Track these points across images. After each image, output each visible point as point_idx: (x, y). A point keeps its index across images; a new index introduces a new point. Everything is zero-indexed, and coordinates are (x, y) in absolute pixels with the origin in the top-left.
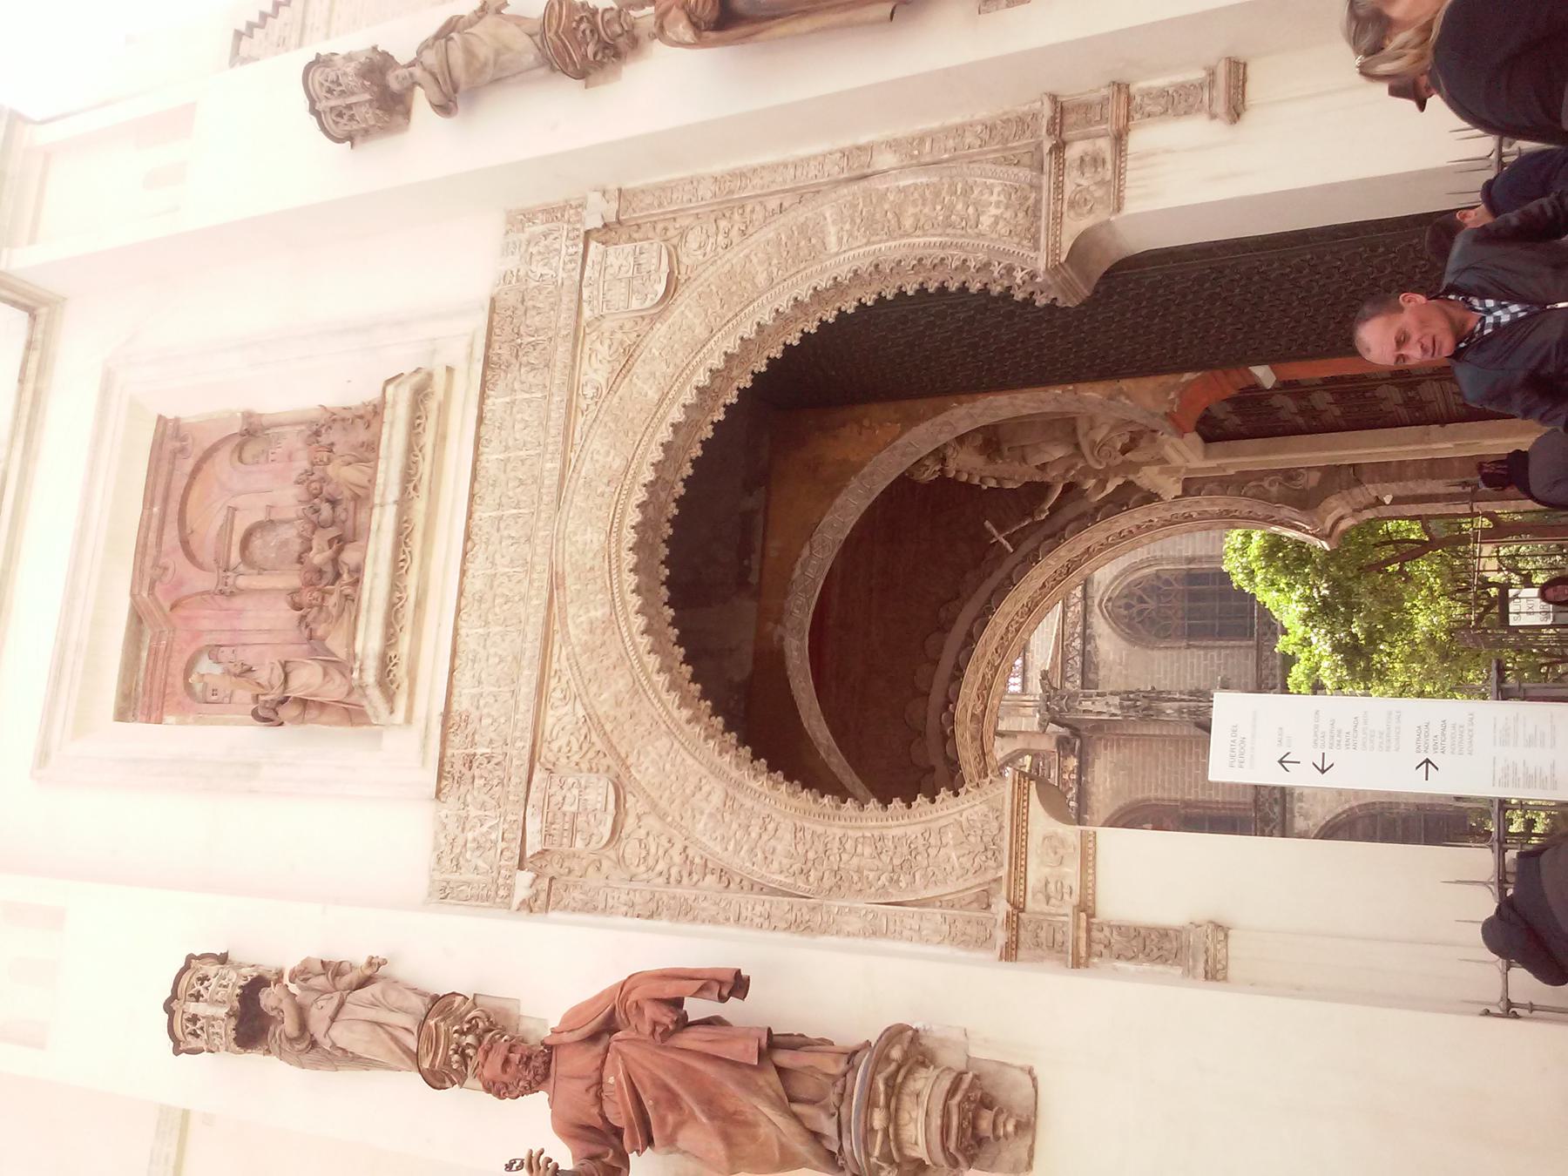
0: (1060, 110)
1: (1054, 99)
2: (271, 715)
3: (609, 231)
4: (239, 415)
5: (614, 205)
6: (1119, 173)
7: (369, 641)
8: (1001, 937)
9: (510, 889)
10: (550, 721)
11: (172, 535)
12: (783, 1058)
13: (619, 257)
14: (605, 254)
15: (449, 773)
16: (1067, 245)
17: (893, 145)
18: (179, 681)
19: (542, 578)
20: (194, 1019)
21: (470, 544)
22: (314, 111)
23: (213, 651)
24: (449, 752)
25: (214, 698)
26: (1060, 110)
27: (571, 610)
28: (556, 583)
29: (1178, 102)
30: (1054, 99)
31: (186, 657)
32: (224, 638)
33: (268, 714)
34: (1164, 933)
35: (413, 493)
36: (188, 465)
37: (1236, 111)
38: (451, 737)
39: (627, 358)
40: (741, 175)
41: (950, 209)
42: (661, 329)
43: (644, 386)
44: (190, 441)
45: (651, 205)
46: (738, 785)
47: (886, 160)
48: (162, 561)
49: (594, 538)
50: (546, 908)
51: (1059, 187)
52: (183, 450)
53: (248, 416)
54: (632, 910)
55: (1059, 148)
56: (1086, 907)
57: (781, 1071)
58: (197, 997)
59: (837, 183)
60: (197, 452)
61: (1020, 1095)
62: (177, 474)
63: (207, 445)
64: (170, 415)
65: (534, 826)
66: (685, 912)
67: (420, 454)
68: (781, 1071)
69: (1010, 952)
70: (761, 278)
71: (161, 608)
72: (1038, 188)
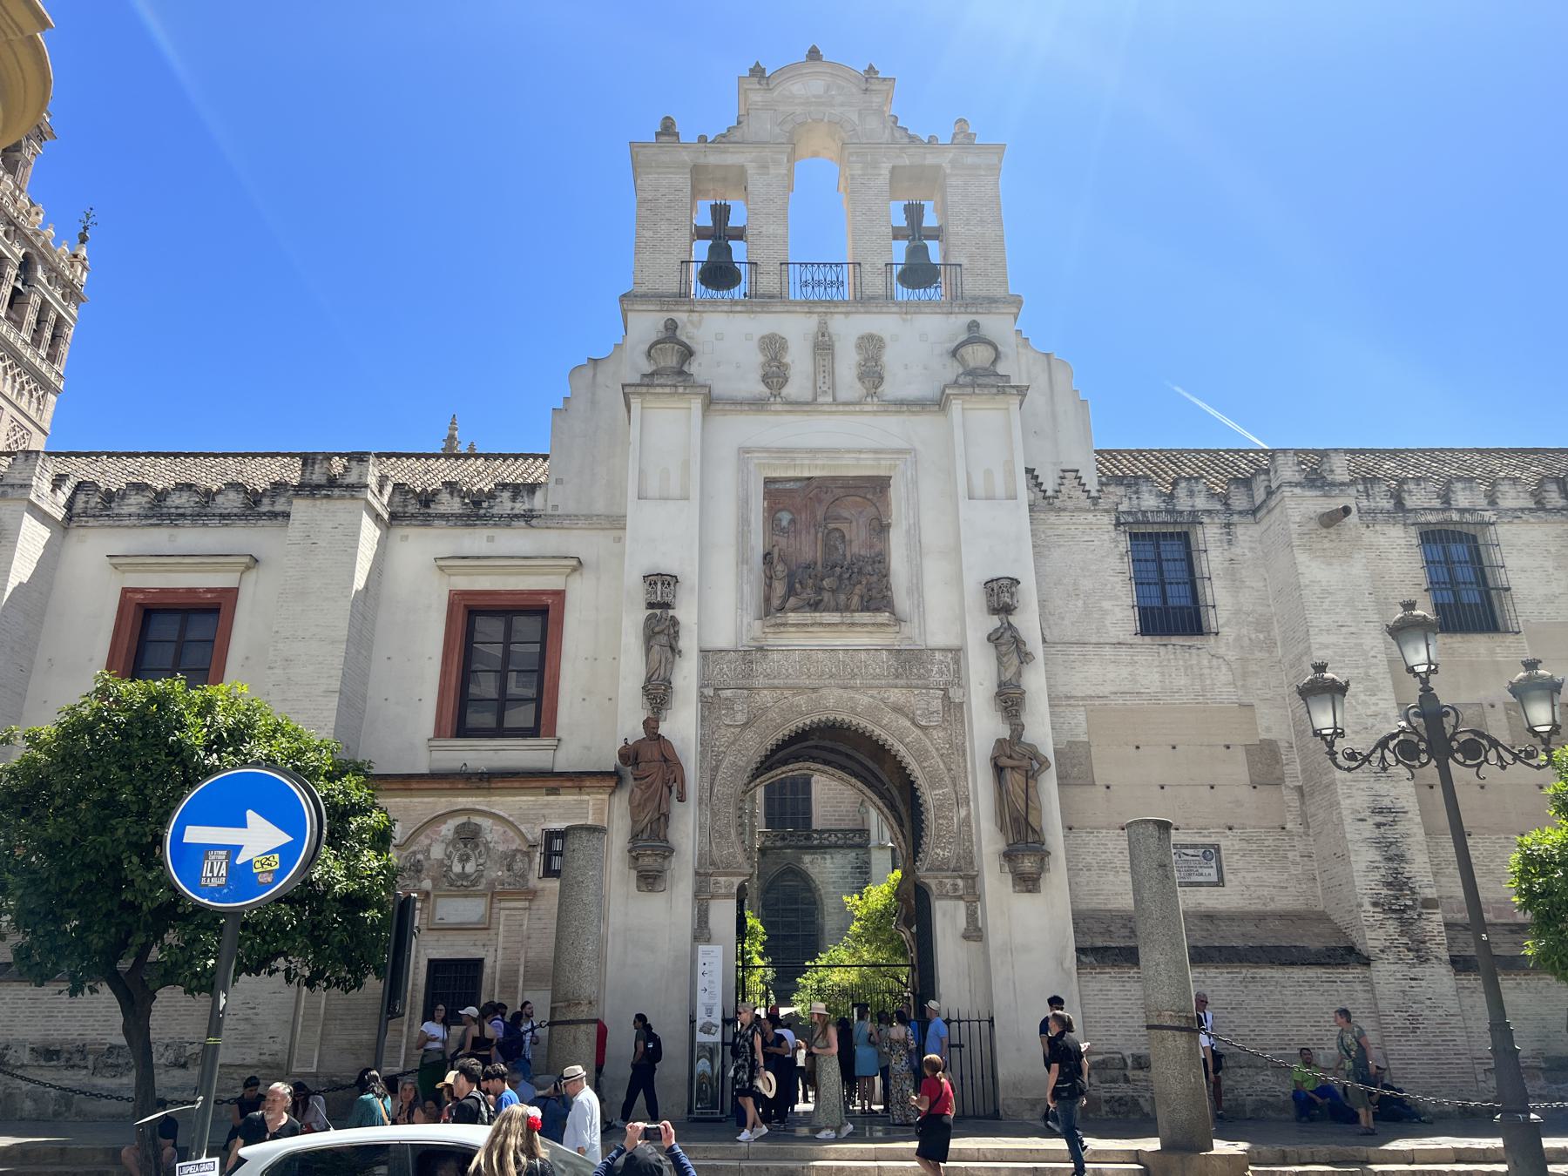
0: (973, 878)
1: (977, 875)
3: (946, 697)
5: (957, 700)
6: (951, 898)
7: (792, 617)
8: (702, 871)
9: (707, 686)
10: (766, 692)
11: (840, 492)
12: (662, 819)
13: (937, 704)
14: (937, 698)
16: (927, 881)
17: (969, 815)
18: (781, 506)
19: (816, 683)
20: (655, 583)
22: (992, 581)
23: (793, 521)
26: (973, 878)
27: (805, 697)
28: (815, 690)
29: (972, 916)
30: (977, 875)
32: (798, 526)
33: (767, 557)
34: (706, 922)
37: (966, 937)
39: (897, 709)
40: (964, 754)
41: (944, 836)
42: (909, 724)
43: (887, 717)
45: (955, 715)
46: (745, 771)
47: (963, 813)
49: (831, 703)
50: (701, 701)
51: (947, 877)
53: (889, 525)
54: (703, 735)
55: (961, 877)
56: (713, 897)
57: (659, 818)
58: (663, 584)
59: (956, 793)
60: (875, 500)
61: (657, 887)
65: (728, 693)
66: (703, 755)
68: (659, 818)
69: (697, 873)
70: (925, 764)
72: (947, 870)
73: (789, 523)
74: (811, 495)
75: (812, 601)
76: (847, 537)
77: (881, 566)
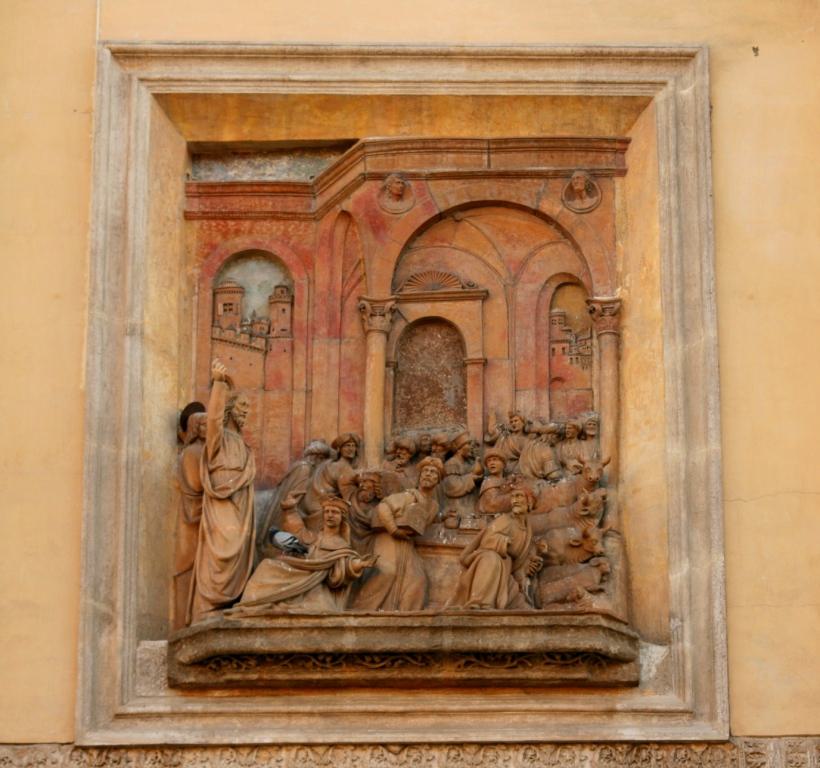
2: (190, 435)
4: (619, 293)
15: (107, 758)
18: (242, 243)
21: (397, 749)
24: (132, 755)
25: (220, 307)
31: (276, 249)
35: (463, 661)
36: (552, 206)
38: (151, 755)
44: (588, 202)
48: (412, 184)
52: (571, 193)
60: (569, 219)
62: (540, 185)
63: (578, 236)
64: (632, 157)
67: (515, 663)
71: (346, 192)
73: (273, 302)
74: (348, 205)
75: (339, 572)
76: (473, 351)
77: (582, 450)
